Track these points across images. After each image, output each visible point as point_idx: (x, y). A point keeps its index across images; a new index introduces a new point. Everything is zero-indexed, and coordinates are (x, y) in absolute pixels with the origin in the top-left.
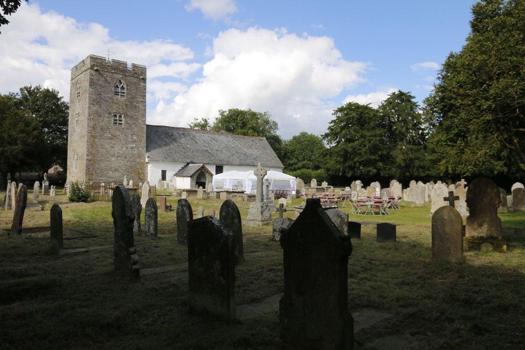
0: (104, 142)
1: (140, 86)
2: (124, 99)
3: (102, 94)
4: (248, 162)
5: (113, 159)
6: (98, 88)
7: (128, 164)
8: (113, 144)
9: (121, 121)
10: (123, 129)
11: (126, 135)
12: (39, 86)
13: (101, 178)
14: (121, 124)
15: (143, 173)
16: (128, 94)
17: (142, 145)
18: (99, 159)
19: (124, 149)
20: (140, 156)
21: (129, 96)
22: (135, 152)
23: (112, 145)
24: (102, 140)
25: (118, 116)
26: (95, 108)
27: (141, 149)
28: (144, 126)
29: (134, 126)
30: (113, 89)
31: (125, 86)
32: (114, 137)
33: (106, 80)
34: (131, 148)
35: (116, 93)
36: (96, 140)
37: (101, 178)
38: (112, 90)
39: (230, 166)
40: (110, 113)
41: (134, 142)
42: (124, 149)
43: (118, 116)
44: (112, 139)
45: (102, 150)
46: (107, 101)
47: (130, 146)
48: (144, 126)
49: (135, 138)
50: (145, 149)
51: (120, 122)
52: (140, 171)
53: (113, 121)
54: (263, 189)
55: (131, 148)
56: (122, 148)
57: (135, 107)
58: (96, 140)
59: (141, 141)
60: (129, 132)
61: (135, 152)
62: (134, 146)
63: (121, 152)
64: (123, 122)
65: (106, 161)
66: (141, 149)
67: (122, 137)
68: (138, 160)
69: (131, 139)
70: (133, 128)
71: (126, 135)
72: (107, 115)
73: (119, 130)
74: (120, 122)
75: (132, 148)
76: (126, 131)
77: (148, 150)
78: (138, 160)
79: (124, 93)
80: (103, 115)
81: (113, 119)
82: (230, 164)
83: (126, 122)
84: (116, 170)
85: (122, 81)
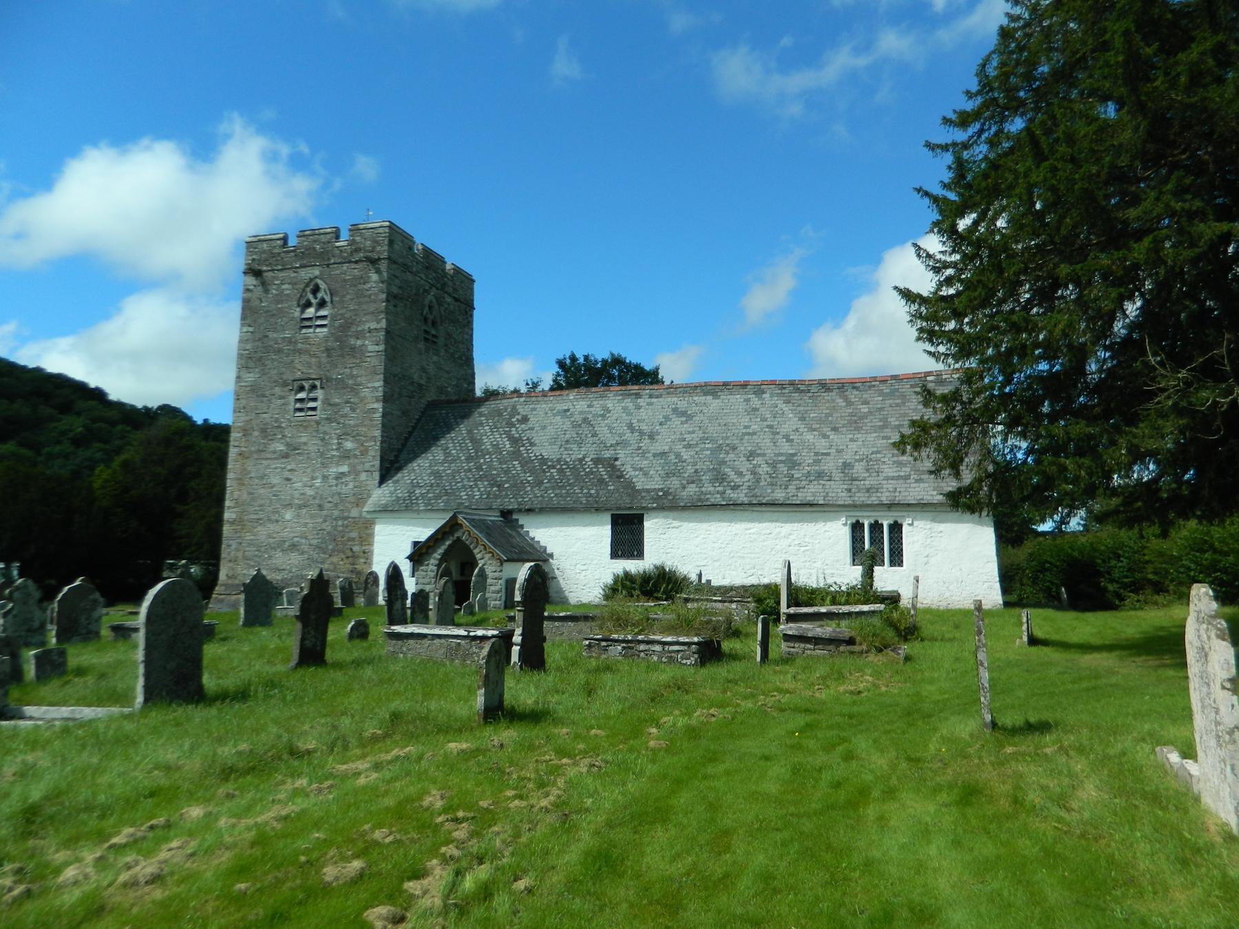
0: (268, 467)
3: (272, 335)
5: (288, 516)
6: (262, 320)
7: (327, 527)
9: (315, 400)
10: (318, 423)
11: (323, 440)
14: (314, 409)
17: (367, 466)
19: (318, 482)
21: (337, 324)
26: (250, 377)
27: (363, 476)
28: (375, 406)
29: (347, 410)
30: (297, 313)
31: (328, 299)
32: (293, 449)
34: (337, 478)
35: (305, 323)
40: (285, 384)
41: (346, 456)
42: (318, 482)
43: (306, 385)
44: (286, 456)
45: (262, 491)
46: (280, 351)
47: (334, 470)
48: (375, 406)
49: (349, 445)
50: (377, 476)
51: (311, 405)
52: (356, 549)
53: (291, 408)
54: (868, 612)
55: (337, 478)
56: (313, 478)
57: (353, 348)
58: (250, 464)
59: (364, 453)
60: (333, 430)
61: (348, 488)
62: (345, 469)
65: (269, 520)
66: (363, 476)
67: (313, 445)
68: (354, 513)
72: (277, 390)
73: (305, 427)
76: (325, 428)
79: (324, 317)
81: (292, 398)
82: (670, 504)
83: (327, 402)
84: (294, 547)
85: (323, 286)
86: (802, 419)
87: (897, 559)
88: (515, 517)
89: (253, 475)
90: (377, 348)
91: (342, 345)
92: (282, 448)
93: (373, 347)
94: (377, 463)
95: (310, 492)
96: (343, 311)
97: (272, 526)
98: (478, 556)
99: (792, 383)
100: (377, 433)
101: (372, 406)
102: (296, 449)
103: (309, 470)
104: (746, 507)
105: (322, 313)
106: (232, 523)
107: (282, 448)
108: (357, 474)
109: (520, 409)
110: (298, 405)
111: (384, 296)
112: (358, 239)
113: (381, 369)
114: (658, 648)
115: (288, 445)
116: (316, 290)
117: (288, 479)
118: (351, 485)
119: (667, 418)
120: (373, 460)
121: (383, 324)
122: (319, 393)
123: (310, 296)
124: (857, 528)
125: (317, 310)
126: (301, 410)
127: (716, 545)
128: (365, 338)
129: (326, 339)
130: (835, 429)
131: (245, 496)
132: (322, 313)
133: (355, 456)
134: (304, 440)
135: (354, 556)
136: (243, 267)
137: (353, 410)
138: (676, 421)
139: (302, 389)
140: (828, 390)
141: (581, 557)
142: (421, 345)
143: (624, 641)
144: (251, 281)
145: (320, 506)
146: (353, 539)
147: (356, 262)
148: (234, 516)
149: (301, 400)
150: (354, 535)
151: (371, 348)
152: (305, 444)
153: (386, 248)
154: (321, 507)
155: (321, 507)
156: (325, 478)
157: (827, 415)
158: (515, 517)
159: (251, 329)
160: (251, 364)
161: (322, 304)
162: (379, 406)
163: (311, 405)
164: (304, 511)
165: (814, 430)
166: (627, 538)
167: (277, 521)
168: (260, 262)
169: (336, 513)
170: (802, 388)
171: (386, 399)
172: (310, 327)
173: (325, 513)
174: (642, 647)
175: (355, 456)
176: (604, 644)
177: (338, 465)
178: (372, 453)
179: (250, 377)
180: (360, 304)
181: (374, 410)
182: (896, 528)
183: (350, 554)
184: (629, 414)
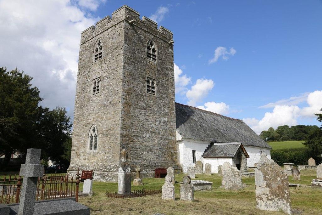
0: (138, 112)
2: (156, 62)
8: (148, 116)
11: (158, 106)
13: (136, 161)
16: (158, 58)
17: (172, 120)
18: (134, 134)
20: (172, 134)
21: (160, 61)
23: (146, 117)
25: (151, 81)
26: (130, 68)
27: (172, 124)
31: (156, 49)
33: (140, 38)
34: (164, 123)
35: (149, 55)
36: (131, 109)
37: (136, 161)
38: (145, 51)
41: (166, 115)
43: (151, 81)
44: (146, 109)
46: (141, 62)
49: (167, 110)
51: (153, 90)
52: (172, 152)
55: (164, 123)
56: (156, 121)
58: (131, 109)
59: (171, 114)
62: (166, 119)
63: (155, 126)
64: (155, 90)
65: (141, 137)
66: (172, 124)
67: (155, 107)
69: (164, 111)
70: (164, 98)
71: (158, 106)
72: (141, 79)
74: (153, 90)
75: (165, 122)
78: (170, 137)
83: (158, 90)
84: (151, 150)
89: (132, 114)
92: (144, 105)
102: (149, 107)
103: (154, 117)
107: (144, 105)
115: (147, 105)
117: (147, 120)
118: (168, 126)
134: (152, 104)
147: (165, 41)
152: (152, 106)
156: (160, 121)
164: (153, 134)
167: (144, 138)
178: (173, 115)
183: (171, 154)
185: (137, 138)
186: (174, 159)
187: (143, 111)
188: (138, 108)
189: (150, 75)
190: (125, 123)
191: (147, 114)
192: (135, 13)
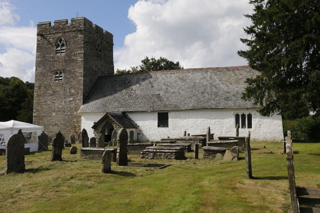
1: (78, 39)
4: (213, 104)
5: (54, 114)
8: (54, 100)
9: (61, 77)
11: (64, 89)
12: (118, 70)
14: (61, 80)
15: (79, 126)
17: (79, 98)
19: (63, 103)
22: (73, 106)
23: (53, 101)
24: (46, 97)
26: (40, 70)
27: (78, 101)
29: (72, 80)
33: (49, 42)
34: (69, 102)
35: (57, 52)
39: (177, 113)
41: (72, 95)
42: (63, 103)
45: (45, 106)
46: (49, 61)
47: (68, 99)
49: (73, 91)
50: (82, 101)
51: (61, 78)
52: (76, 125)
53: (54, 79)
55: (69, 102)
56: (61, 102)
57: (73, 60)
58: (41, 98)
60: (67, 86)
61: (73, 106)
62: (71, 99)
65: (48, 116)
66: (78, 101)
70: (71, 82)
71: (64, 89)
75: (70, 101)
77: (84, 103)
78: (75, 113)
79: (64, 49)
80: (46, 75)
81: (54, 76)
82: (177, 110)
83: (65, 77)
84: (56, 124)
85: (63, 39)
86: (220, 80)
87: (250, 126)
88: (127, 114)
89: (42, 101)
90: (81, 60)
91: (69, 60)
92: (51, 92)
93: (80, 59)
94: (82, 97)
95: (61, 107)
96: (70, 47)
97: (49, 118)
98: (115, 127)
99: (217, 68)
100: (82, 87)
101: (80, 78)
102: (55, 93)
104: (201, 110)
105: (64, 48)
106: (36, 117)
108: (76, 100)
109: (128, 78)
110: (56, 79)
111: (83, 42)
112: (74, 23)
113: (82, 66)
114: (163, 154)
115: (53, 92)
116: (61, 41)
117: (54, 103)
118: (74, 104)
119: (176, 81)
120: (80, 97)
121: (83, 51)
122: (63, 75)
123: (59, 43)
124: (237, 116)
125: (61, 48)
126: (57, 80)
127: (191, 122)
128: (77, 56)
129: (65, 57)
130: (231, 84)
131: (39, 108)
132: (64, 48)
133: (75, 95)
134: (58, 90)
135: (75, 127)
136: (36, 33)
137: (74, 80)
138: (179, 82)
139: (57, 73)
140: (229, 71)
141: (149, 128)
142: (96, 58)
143: (153, 152)
144: (40, 37)
145: (64, 111)
146: (75, 122)
147: (74, 31)
148: (36, 115)
149: (57, 77)
150: (75, 120)
151: (79, 59)
153: (83, 26)
154: (64, 112)
155: (64, 112)
156: (65, 102)
157: (229, 79)
158: (127, 114)
159: (40, 54)
160: (40, 65)
161: (63, 45)
162: (82, 78)
163: (61, 78)
165: (224, 84)
166: (163, 121)
168: (42, 31)
169: (69, 113)
170: (221, 70)
171: (84, 76)
172: (59, 53)
173: (65, 113)
174: (159, 154)
175: (75, 95)
176: (147, 153)
177: (69, 98)
178: (80, 94)
179: (40, 70)
180: (75, 45)
181: (81, 80)
182: (250, 117)
183: (74, 127)
184: (164, 80)
185: (45, 117)
186: (77, 131)
187: (50, 98)
188: (46, 96)
189: (57, 68)
190: (36, 108)
191: (53, 99)
192: (45, 24)
